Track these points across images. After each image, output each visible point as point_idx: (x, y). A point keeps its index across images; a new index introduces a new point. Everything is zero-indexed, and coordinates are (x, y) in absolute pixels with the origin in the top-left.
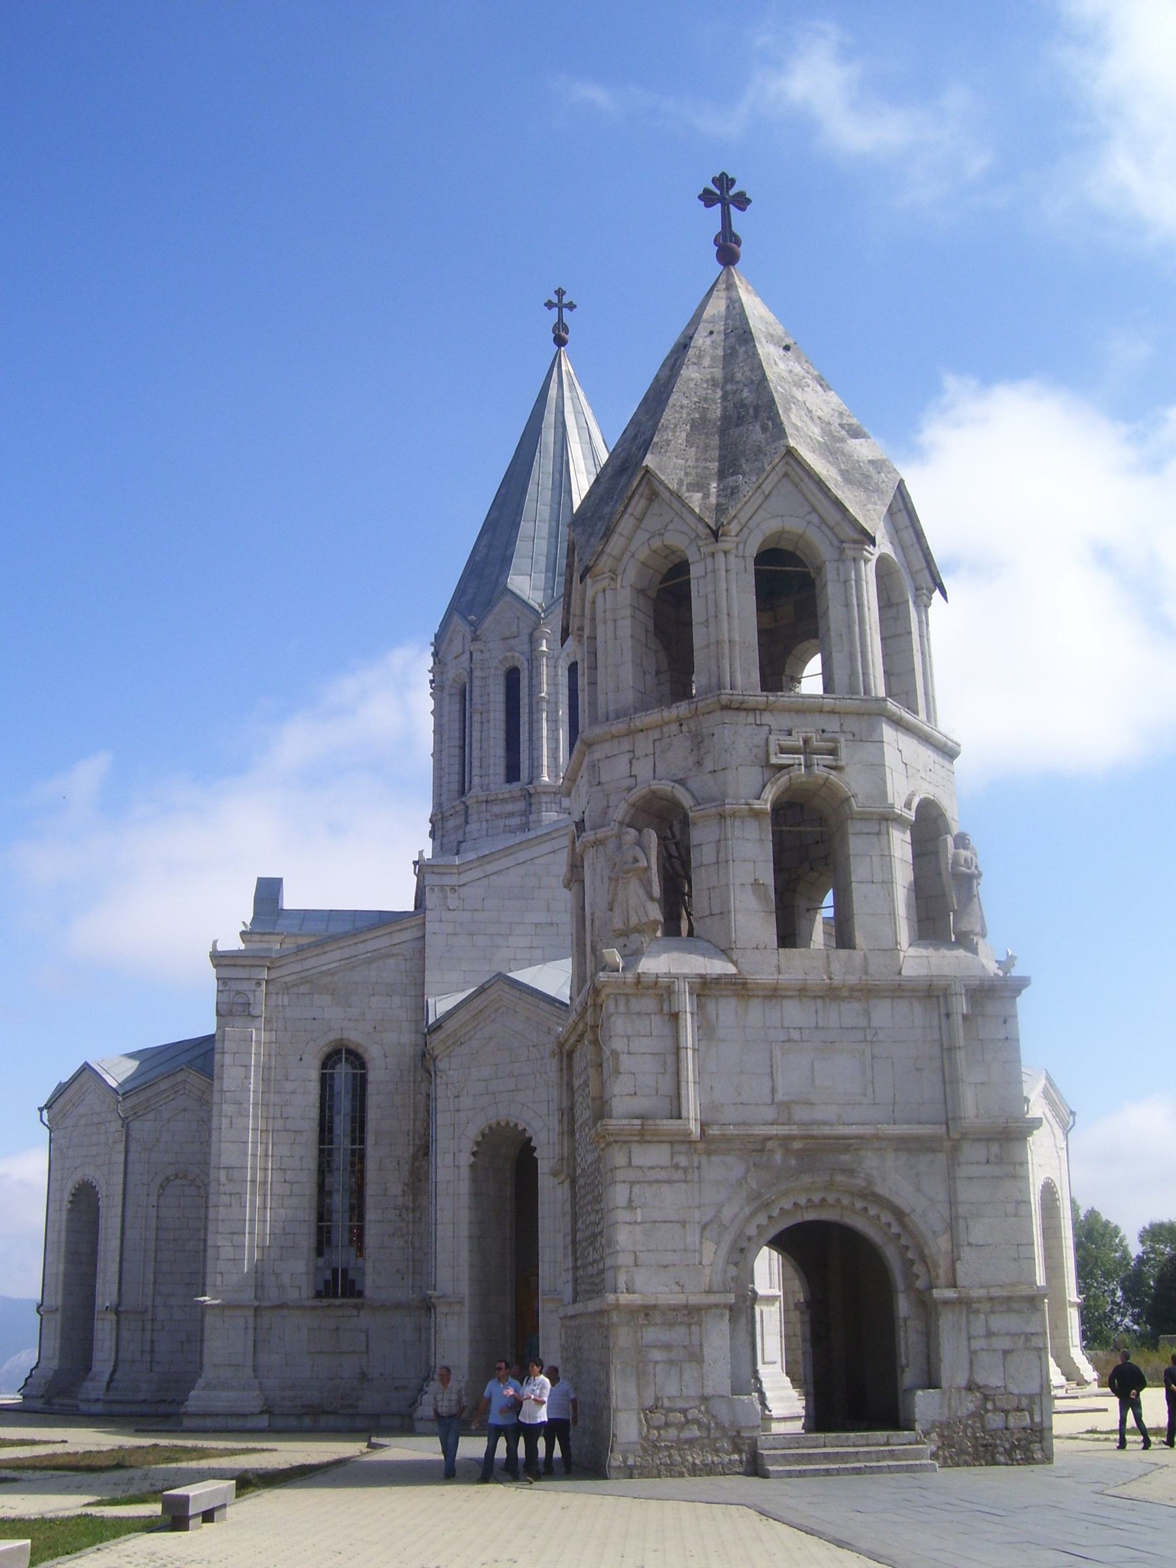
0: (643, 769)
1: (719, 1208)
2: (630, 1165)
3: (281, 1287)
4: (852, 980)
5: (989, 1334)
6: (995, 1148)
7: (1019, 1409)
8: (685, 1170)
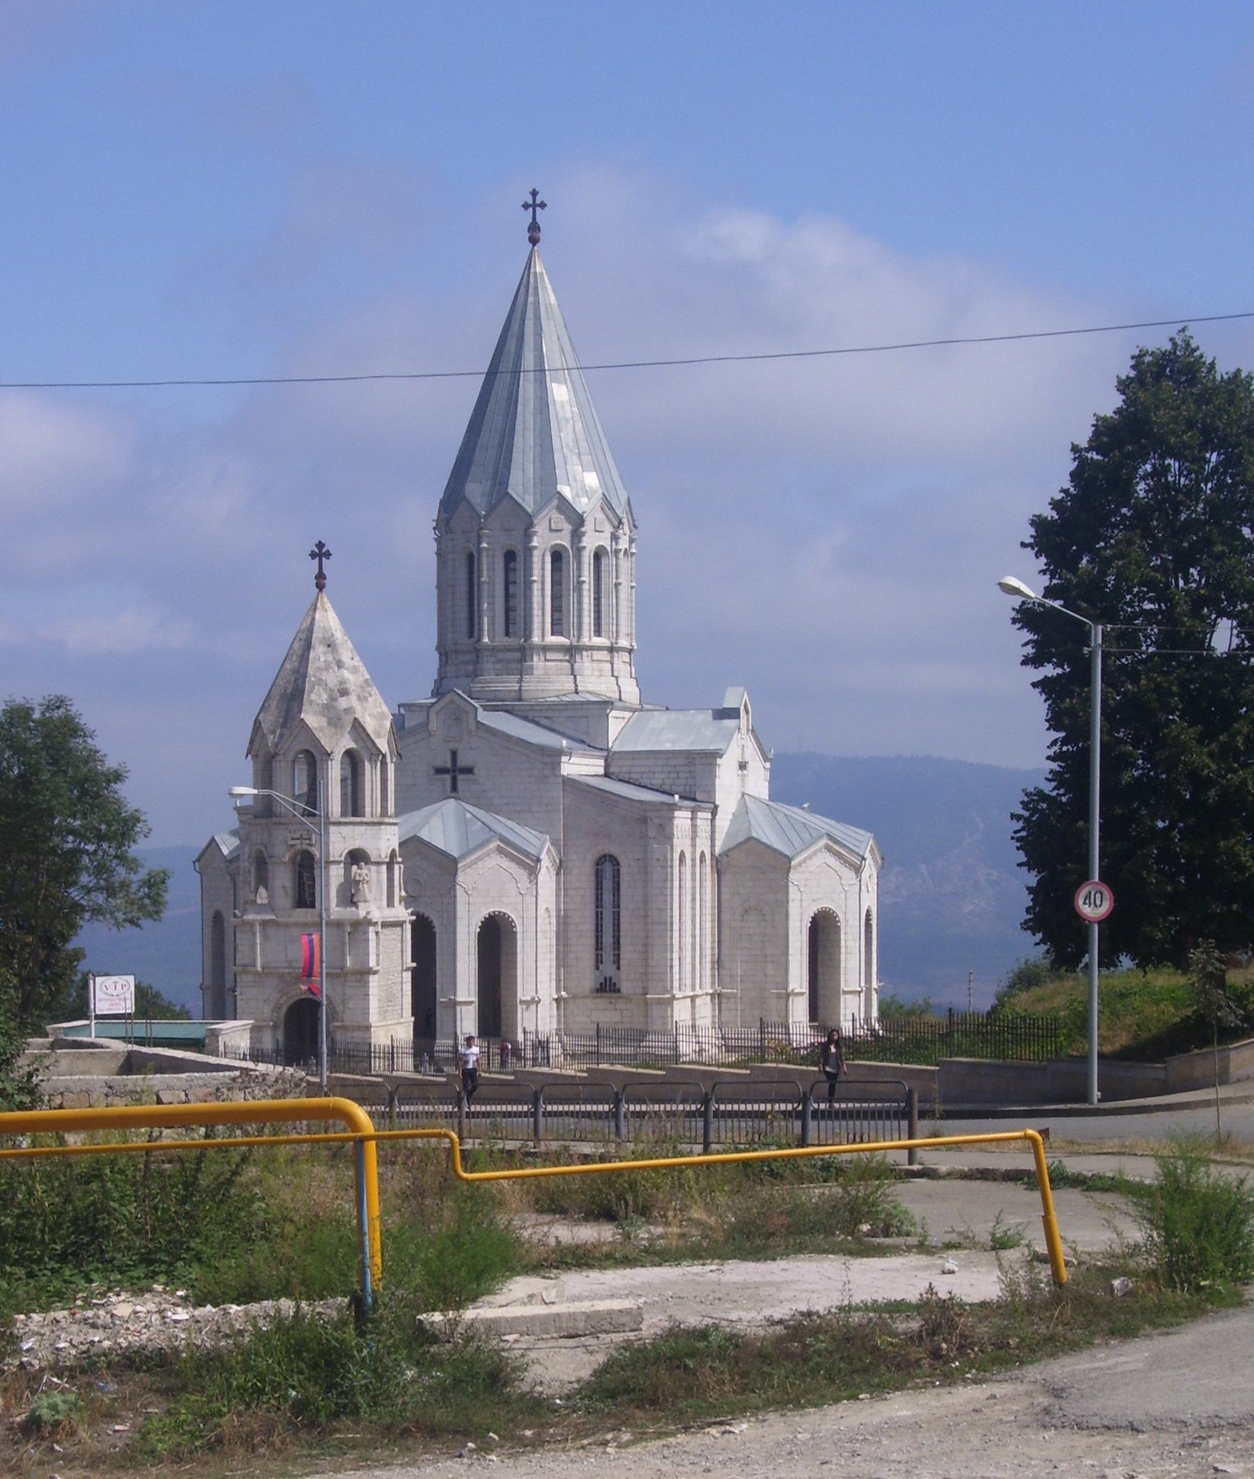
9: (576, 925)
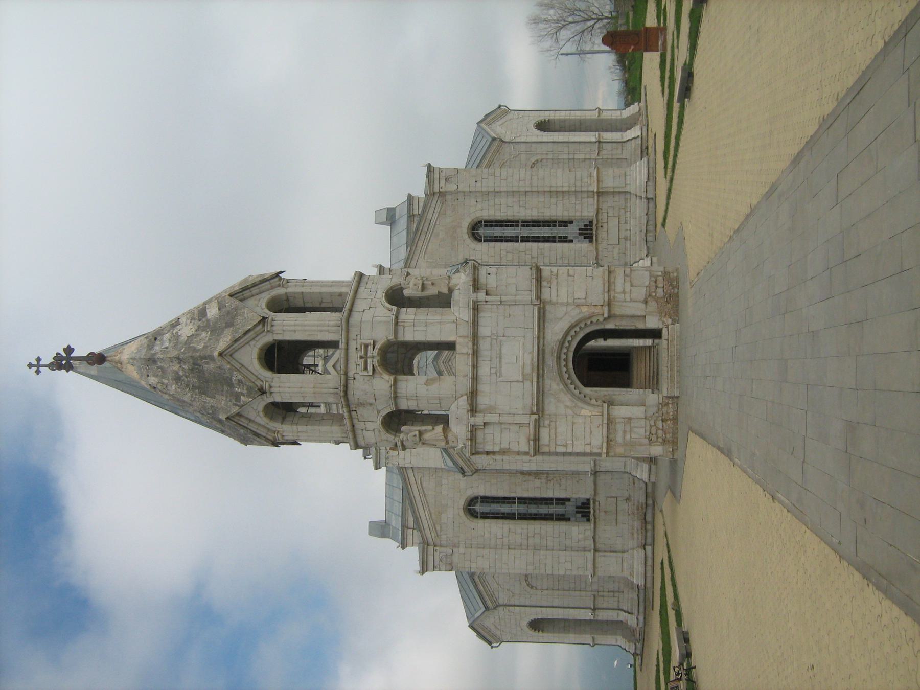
0: (371, 426)
1: (567, 407)
2: (549, 445)
3: (585, 539)
4: (470, 344)
5: (624, 292)
6: (544, 284)
7: (656, 282)
8: (551, 421)
9: (532, 258)
